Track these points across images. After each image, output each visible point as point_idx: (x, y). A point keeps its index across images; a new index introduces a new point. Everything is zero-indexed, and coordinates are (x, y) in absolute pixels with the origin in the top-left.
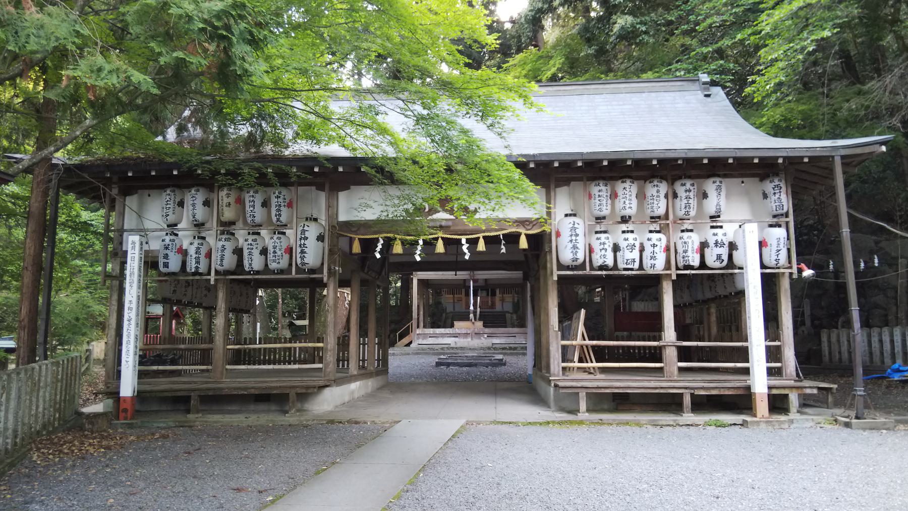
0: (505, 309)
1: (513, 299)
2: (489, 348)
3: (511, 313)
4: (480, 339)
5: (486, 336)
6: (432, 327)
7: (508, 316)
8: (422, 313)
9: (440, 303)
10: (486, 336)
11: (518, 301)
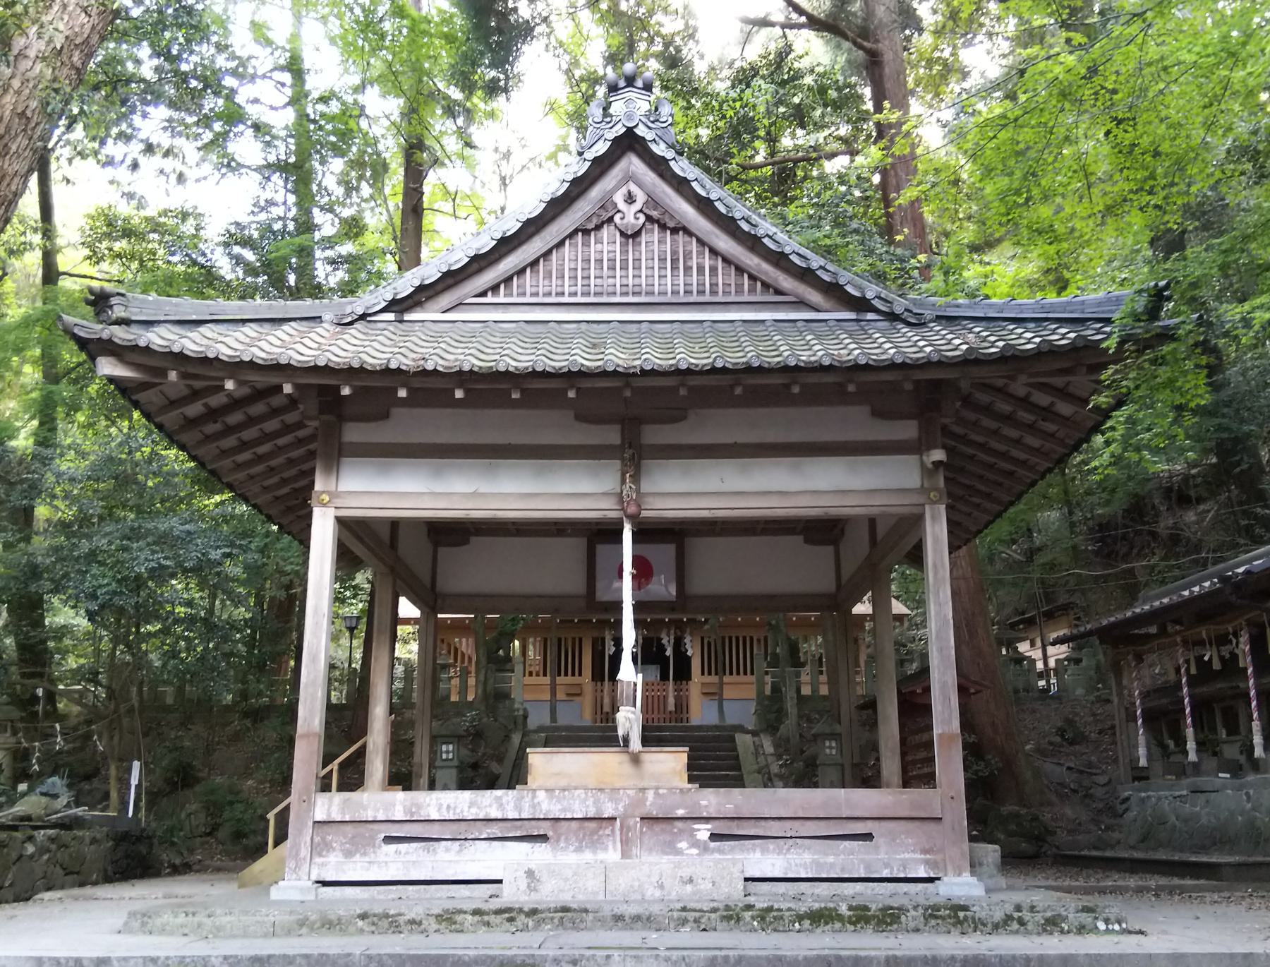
0: (731, 720)
1: (761, 684)
2: (731, 916)
3: (754, 733)
4: (670, 848)
5: (703, 832)
6: (464, 785)
7: (744, 741)
8: (143, 804)
9: (503, 696)
10: (703, 832)
11: (776, 689)
